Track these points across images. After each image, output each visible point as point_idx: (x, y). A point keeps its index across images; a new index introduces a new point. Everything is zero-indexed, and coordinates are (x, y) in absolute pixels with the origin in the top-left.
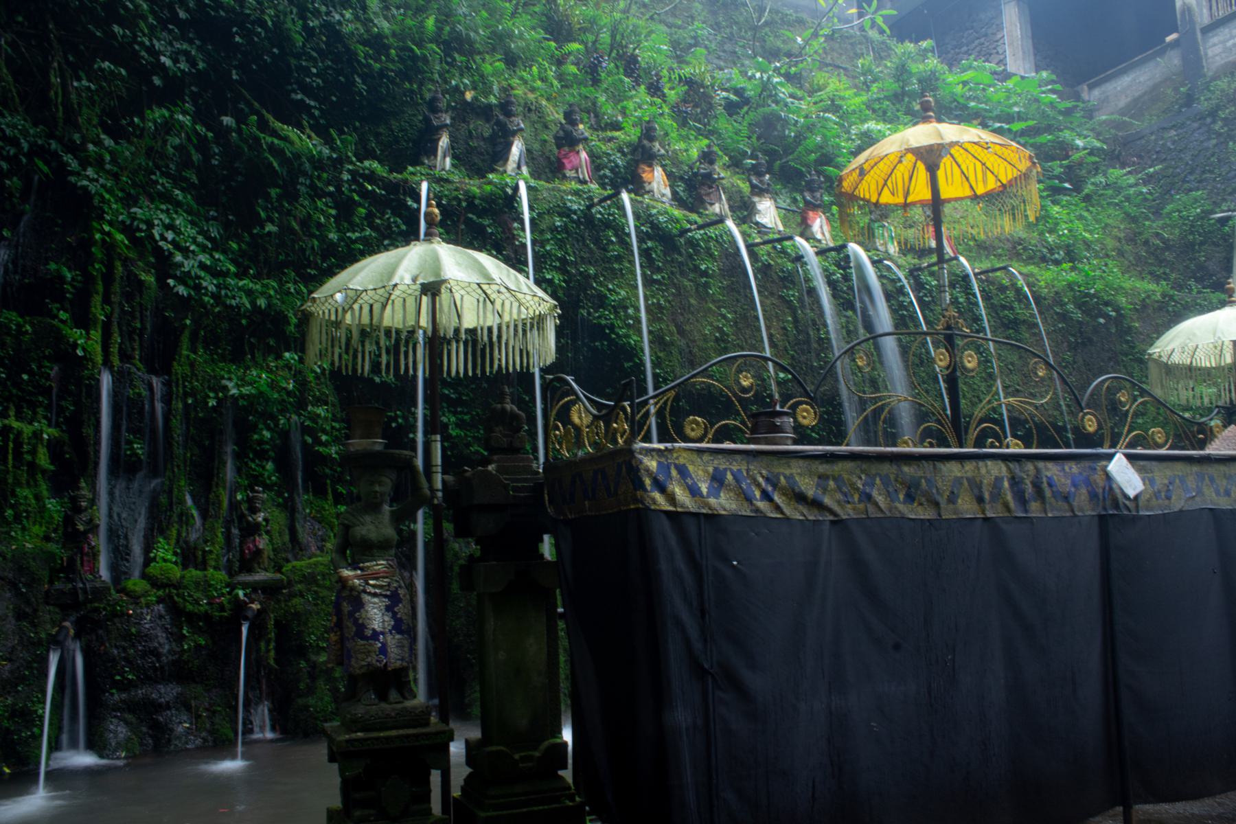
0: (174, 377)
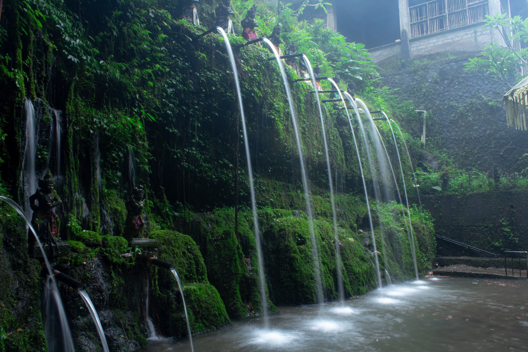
0: (67, 112)
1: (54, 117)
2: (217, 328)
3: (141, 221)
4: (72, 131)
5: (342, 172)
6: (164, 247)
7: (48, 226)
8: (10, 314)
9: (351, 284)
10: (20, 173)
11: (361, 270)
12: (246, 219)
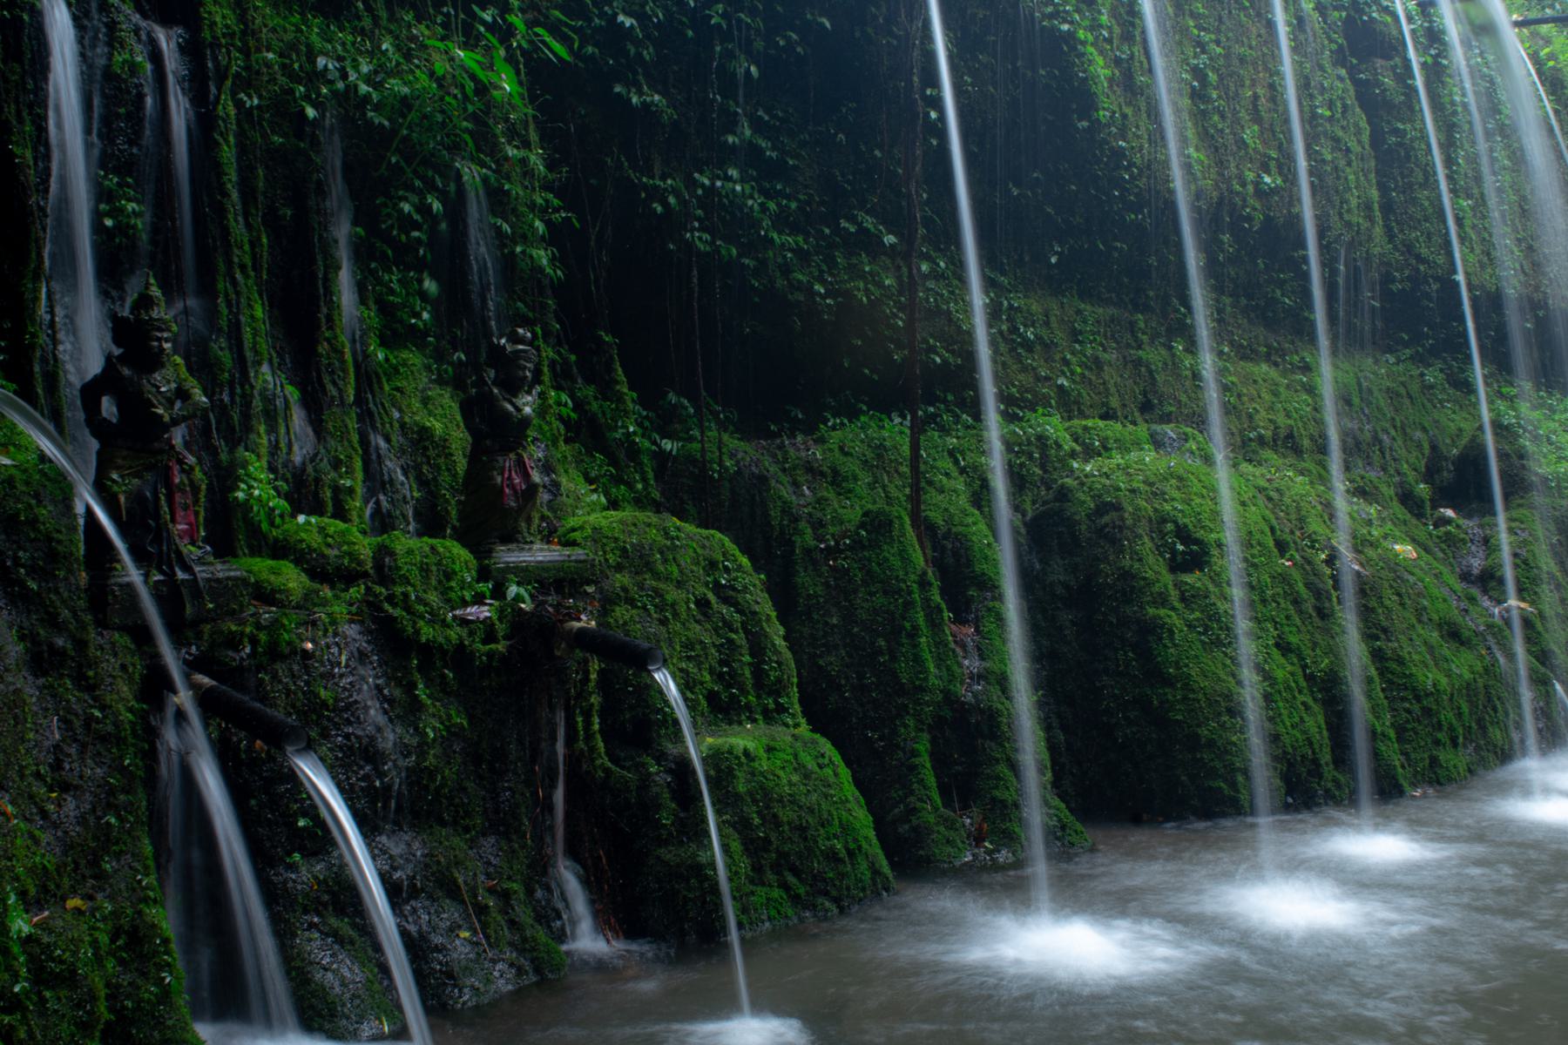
0: (207, 34)
1: (156, 57)
2: (842, 910)
3: (526, 476)
4: (232, 111)
5: (1368, 259)
6: (622, 579)
7: (157, 499)
8: (36, 842)
9: (1400, 740)
10: (36, 290)
11: (1444, 681)
12: (956, 462)
